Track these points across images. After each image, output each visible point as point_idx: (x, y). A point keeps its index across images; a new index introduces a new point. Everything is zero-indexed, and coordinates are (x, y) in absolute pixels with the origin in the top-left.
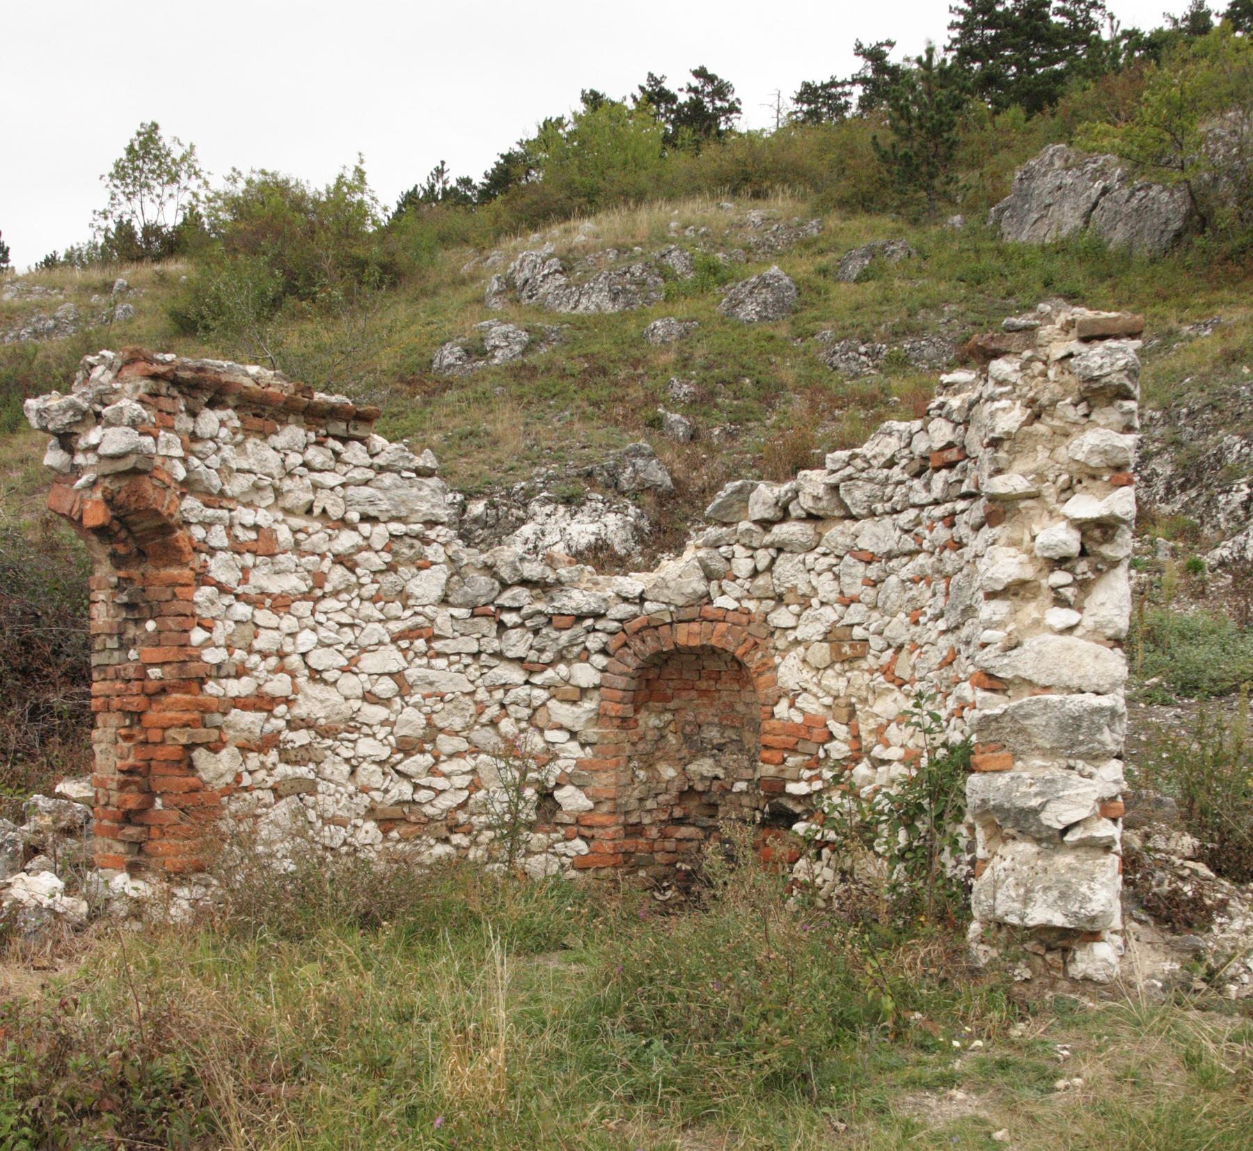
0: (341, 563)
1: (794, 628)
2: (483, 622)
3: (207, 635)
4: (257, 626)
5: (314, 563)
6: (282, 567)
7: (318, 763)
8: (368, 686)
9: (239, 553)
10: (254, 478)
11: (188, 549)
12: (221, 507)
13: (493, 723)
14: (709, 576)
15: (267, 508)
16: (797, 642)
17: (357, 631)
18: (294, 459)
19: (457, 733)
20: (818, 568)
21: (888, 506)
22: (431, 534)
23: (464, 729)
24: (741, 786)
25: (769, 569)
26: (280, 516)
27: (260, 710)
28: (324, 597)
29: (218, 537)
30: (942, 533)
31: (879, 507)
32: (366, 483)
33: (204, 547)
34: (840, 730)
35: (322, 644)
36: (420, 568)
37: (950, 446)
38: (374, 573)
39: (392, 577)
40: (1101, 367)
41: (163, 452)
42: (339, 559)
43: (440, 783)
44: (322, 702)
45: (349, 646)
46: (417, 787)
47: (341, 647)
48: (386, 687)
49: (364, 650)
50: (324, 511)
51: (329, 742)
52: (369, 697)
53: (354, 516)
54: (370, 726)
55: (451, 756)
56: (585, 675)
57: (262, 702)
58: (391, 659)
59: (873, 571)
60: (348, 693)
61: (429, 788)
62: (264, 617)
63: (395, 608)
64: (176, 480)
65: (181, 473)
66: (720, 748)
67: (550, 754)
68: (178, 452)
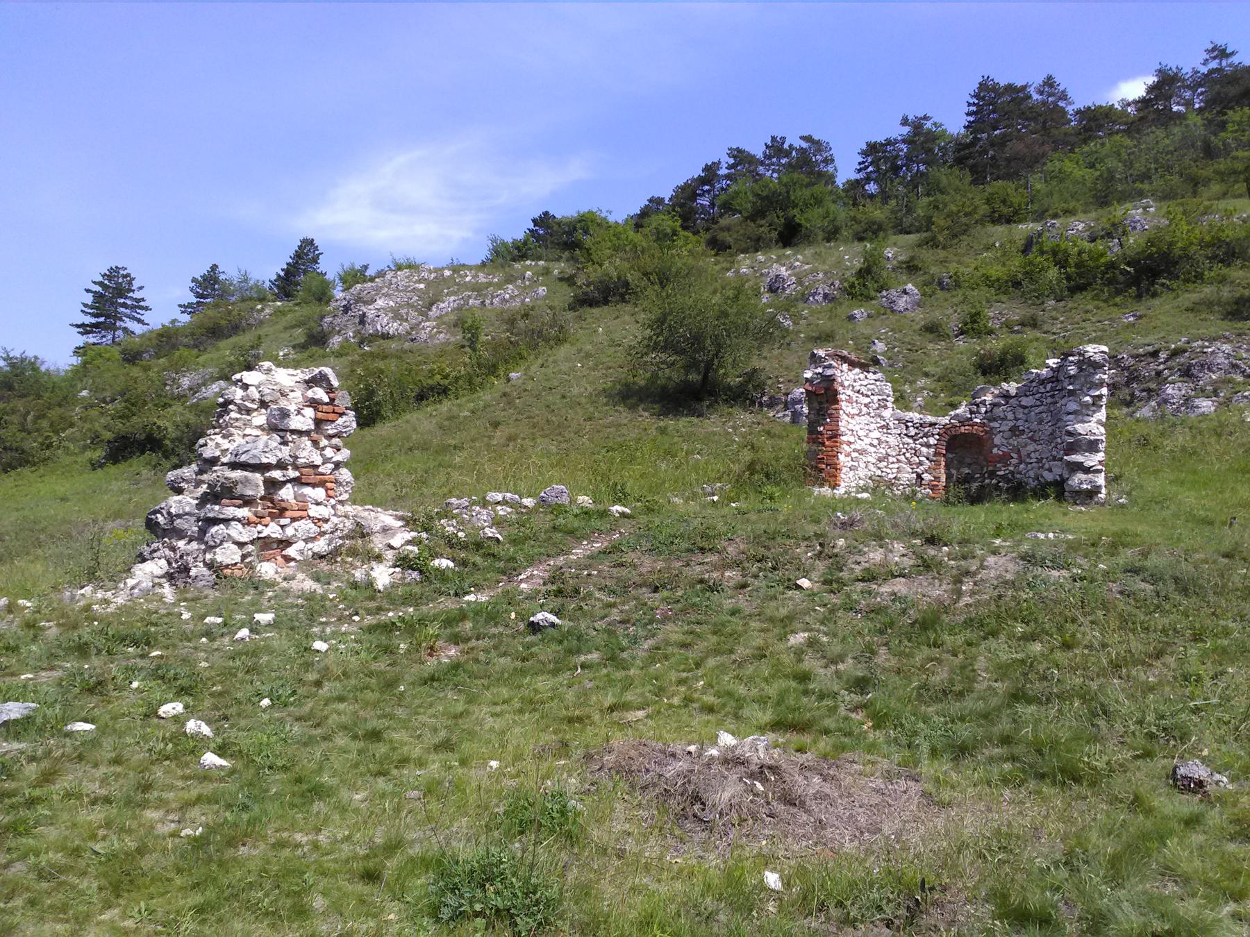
13: (904, 454)
14: (971, 412)
30: (1049, 400)
34: (1015, 456)
42: (866, 405)
43: (889, 471)
48: (876, 442)
52: (871, 445)
53: (869, 393)
56: (932, 441)
58: (876, 434)
59: (1026, 411)
63: (878, 420)
66: (970, 464)
67: (920, 464)
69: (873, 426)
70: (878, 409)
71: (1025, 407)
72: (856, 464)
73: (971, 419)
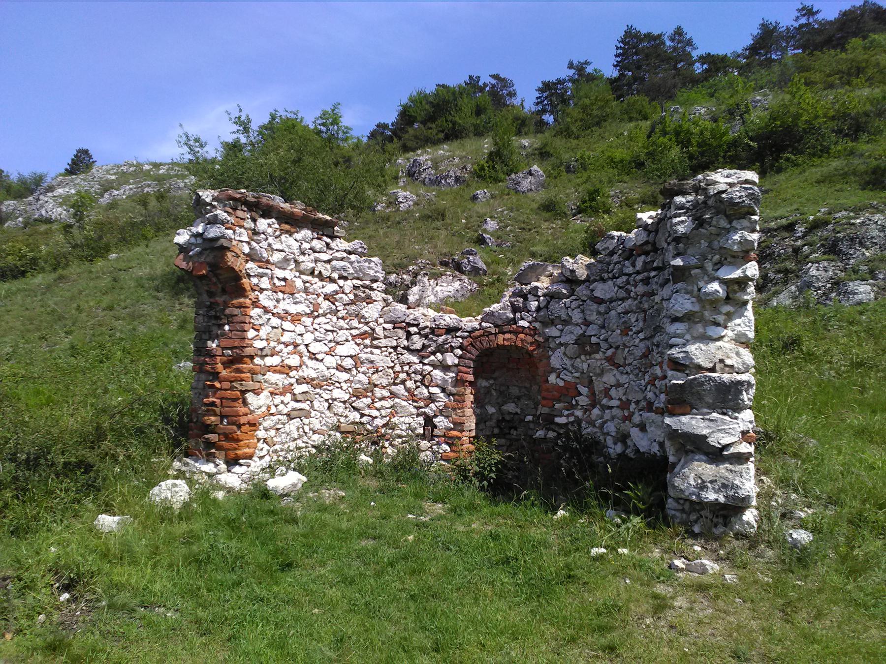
0: (328, 299)
1: (559, 337)
2: (400, 331)
3: (257, 333)
4: (283, 330)
7: (311, 402)
8: (339, 362)
9: (276, 292)
10: (283, 254)
11: (248, 288)
13: (403, 382)
14: (515, 309)
15: (291, 270)
16: (561, 344)
17: (335, 334)
18: (306, 246)
19: (384, 388)
20: (573, 306)
21: (610, 275)
22: (375, 285)
23: (388, 385)
24: (529, 418)
25: (547, 307)
26: (297, 274)
27: (283, 373)
28: (318, 316)
29: (265, 283)
30: (641, 289)
31: (606, 276)
32: (342, 259)
34: (584, 390)
35: (316, 340)
36: (368, 303)
37: (647, 243)
38: (345, 305)
39: (354, 307)
40: (740, 198)
41: (238, 238)
42: (327, 297)
43: (375, 413)
45: (330, 341)
46: (362, 415)
47: (326, 342)
48: (348, 363)
49: (338, 343)
50: (320, 272)
51: (318, 390)
52: (340, 368)
53: (335, 275)
54: (340, 383)
55: (380, 399)
56: (451, 359)
57: (285, 369)
58: (350, 348)
59: (602, 308)
60: (329, 365)
61: (369, 416)
62: (287, 325)
63: (355, 323)
64: (244, 253)
65: (246, 250)
66: (519, 398)
67: (431, 399)
68: (245, 238)
69: (343, 335)
70: (352, 303)
71: (599, 301)
72: (305, 406)
73: (514, 321)
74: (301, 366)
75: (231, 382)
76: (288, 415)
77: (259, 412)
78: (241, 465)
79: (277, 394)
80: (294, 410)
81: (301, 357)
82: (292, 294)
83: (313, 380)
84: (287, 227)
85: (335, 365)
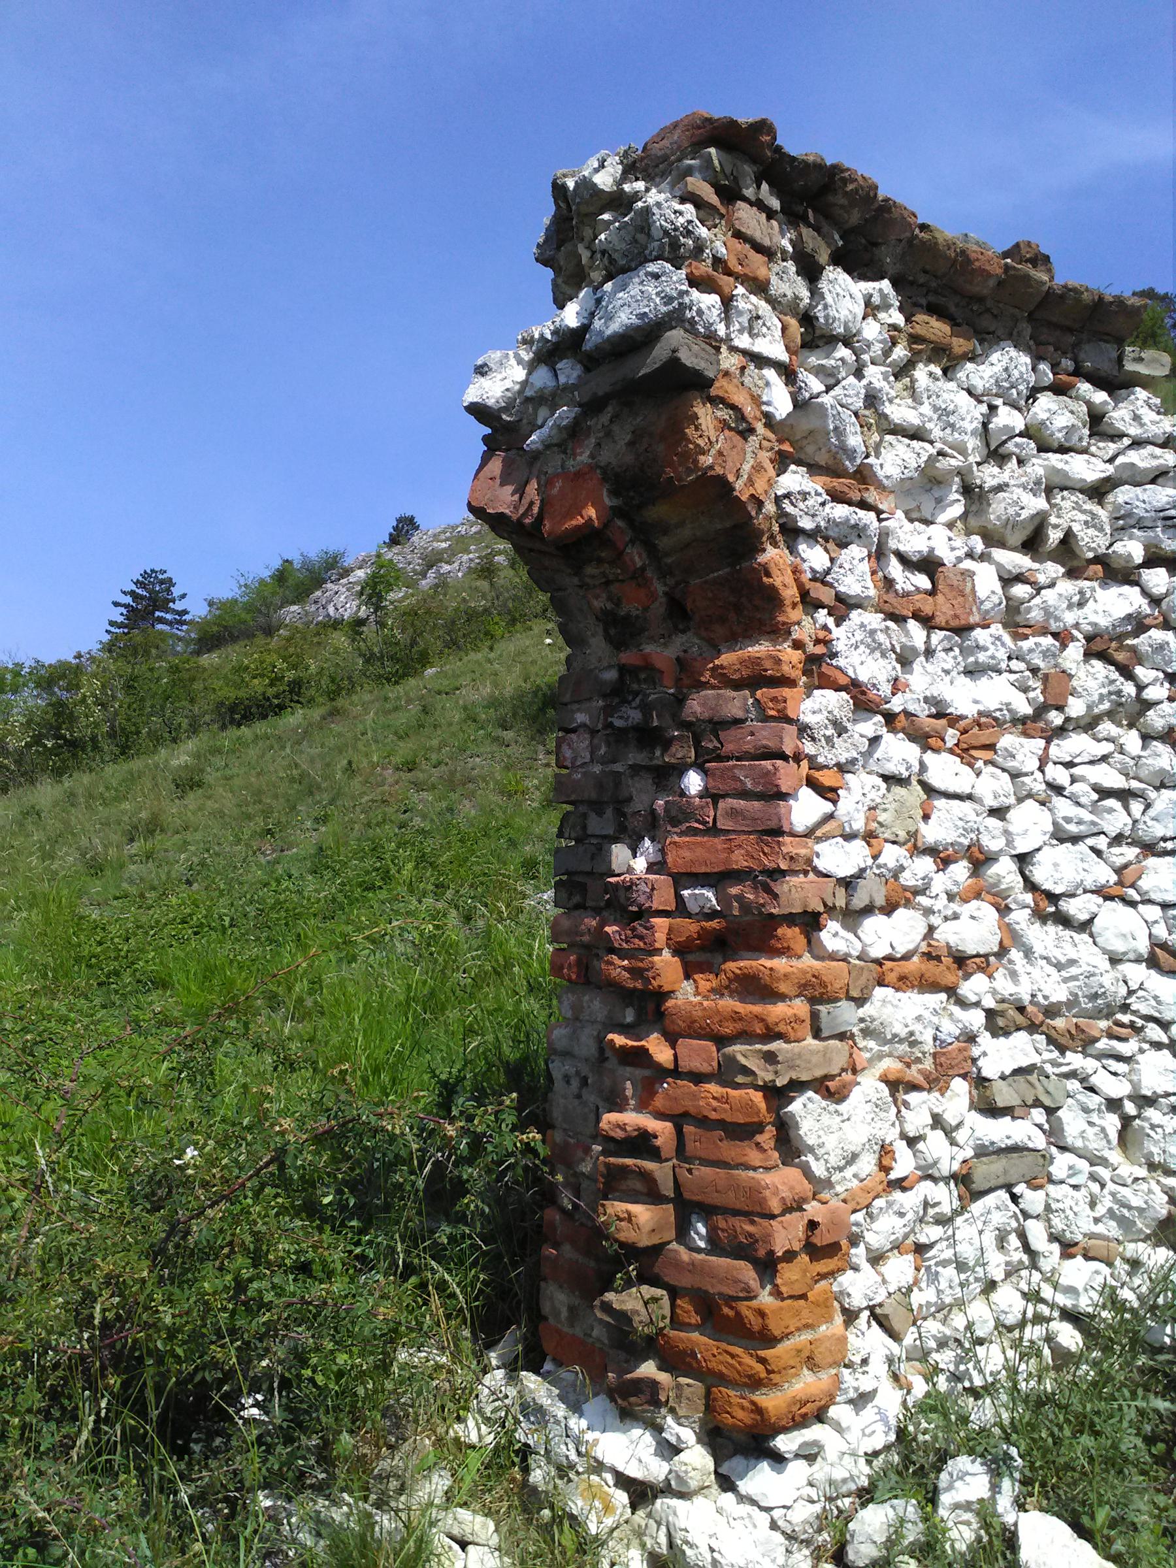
0: (1104, 656)
3: (827, 807)
5: (1046, 654)
6: (982, 657)
7: (1051, 1111)
9: (899, 619)
10: (927, 450)
11: (790, 593)
12: (864, 505)
15: (950, 525)
17: (1136, 807)
18: (1008, 418)
26: (978, 543)
27: (928, 985)
28: (1061, 731)
33: (826, 596)
35: (1061, 836)
41: (743, 341)
44: (1059, 966)
45: (1117, 840)
47: (1102, 842)
49: (1150, 848)
50: (1068, 538)
51: (1075, 1060)
60: (1119, 946)
64: (768, 418)
74: (1002, 951)
75: (721, 1041)
76: (962, 1179)
77: (846, 1182)
78: (778, 1459)
79: (914, 1087)
80: (983, 1151)
81: (1004, 910)
82: (962, 630)
83: (1052, 1011)
84: (936, 328)
85: (1143, 947)
